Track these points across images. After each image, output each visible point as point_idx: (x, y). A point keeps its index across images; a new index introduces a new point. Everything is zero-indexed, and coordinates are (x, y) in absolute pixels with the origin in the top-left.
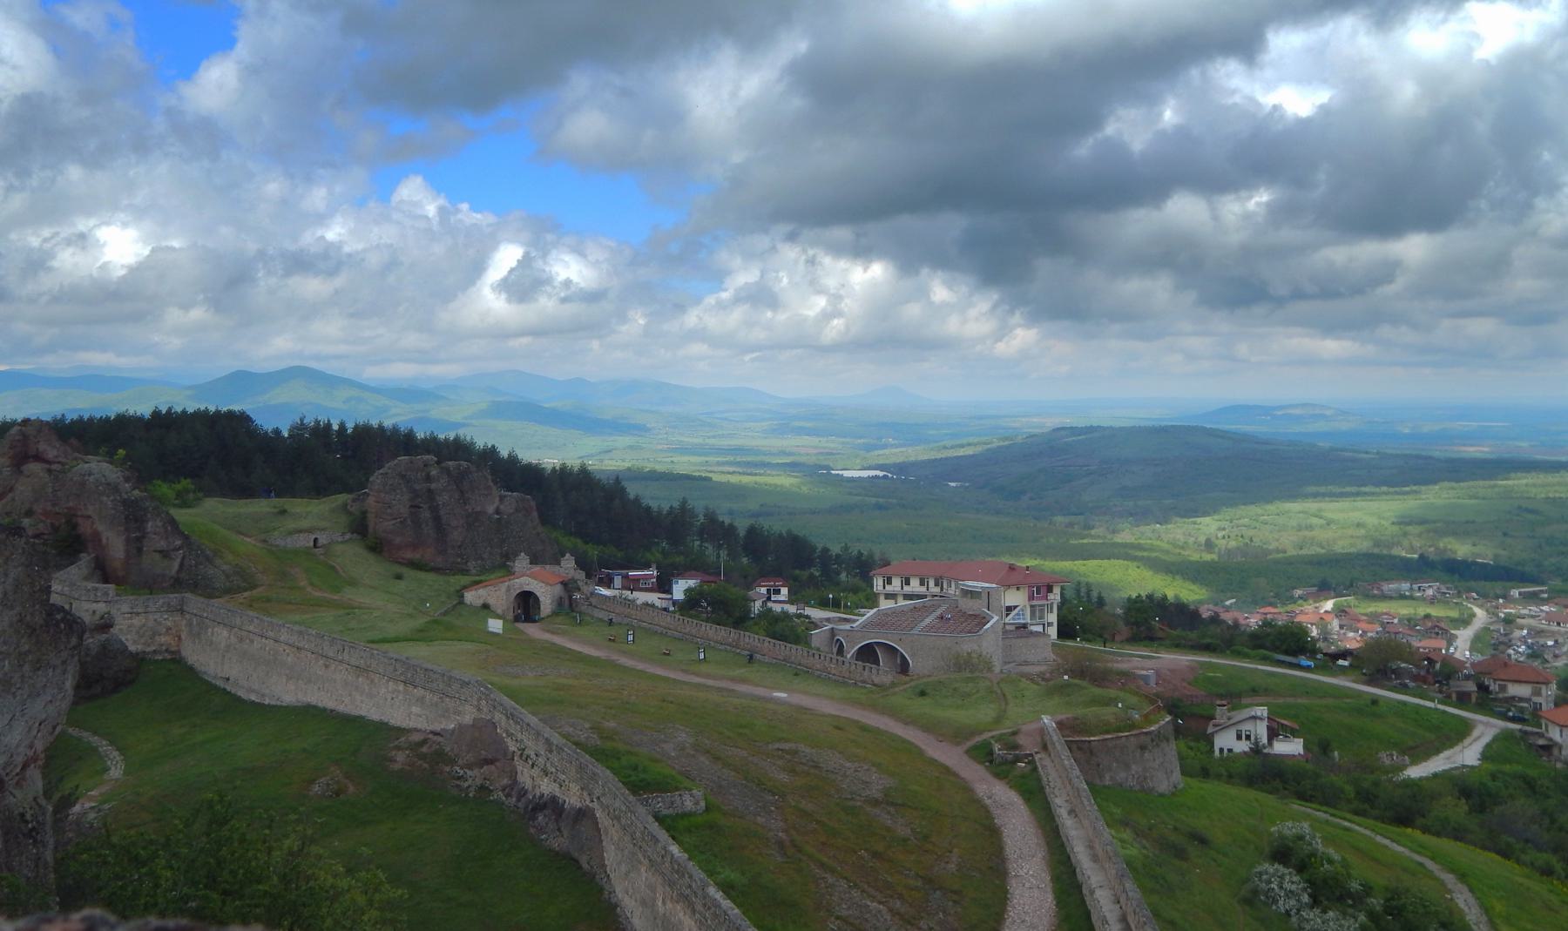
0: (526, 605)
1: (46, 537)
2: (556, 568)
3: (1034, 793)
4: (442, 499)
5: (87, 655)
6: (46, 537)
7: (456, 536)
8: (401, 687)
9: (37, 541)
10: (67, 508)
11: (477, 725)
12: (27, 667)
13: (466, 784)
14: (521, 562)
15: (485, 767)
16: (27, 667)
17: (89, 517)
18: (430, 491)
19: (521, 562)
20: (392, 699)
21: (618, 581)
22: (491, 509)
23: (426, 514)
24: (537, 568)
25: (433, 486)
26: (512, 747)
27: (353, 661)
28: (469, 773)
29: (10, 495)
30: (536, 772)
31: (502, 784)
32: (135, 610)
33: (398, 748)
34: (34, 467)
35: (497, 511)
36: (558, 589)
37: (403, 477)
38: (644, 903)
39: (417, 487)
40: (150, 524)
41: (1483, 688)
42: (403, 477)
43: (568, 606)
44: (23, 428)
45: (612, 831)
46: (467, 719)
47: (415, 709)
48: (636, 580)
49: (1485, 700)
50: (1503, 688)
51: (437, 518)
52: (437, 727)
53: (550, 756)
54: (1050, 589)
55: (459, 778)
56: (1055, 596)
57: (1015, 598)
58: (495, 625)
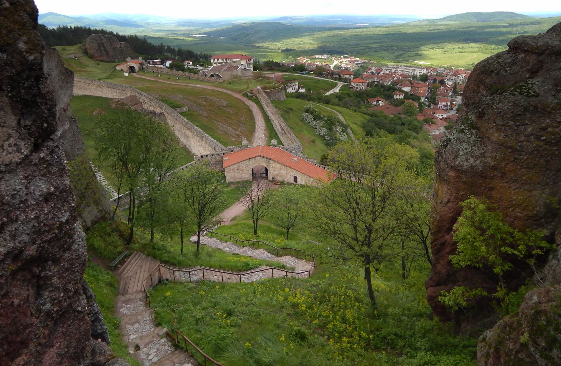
0: (132, 69)
2: (138, 60)
3: (258, 102)
4: (106, 44)
7: (111, 53)
8: (110, 89)
11: (131, 96)
12: (65, 83)
14: (129, 59)
16: (65, 83)
18: (102, 42)
19: (129, 59)
21: (151, 63)
22: (118, 47)
23: (102, 48)
24: (133, 60)
25: (103, 41)
26: (141, 101)
27: (96, 84)
30: (148, 106)
33: (112, 103)
35: (120, 47)
36: (139, 65)
37: (95, 39)
38: (179, 131)
39: (99, 42)
41: (340, 76)
42: (95, 39)
43: (142, 69)
45: (169, 117)
46: (129, 95)
47: (114, 94)
48: (156, 62)
49: (340, 79)
50: (344, 76)
51: (105, 49)
52: (121, 98)
54: (251, 60)
56: (252, 61)
57: (243, 62)
58: (126, 74)
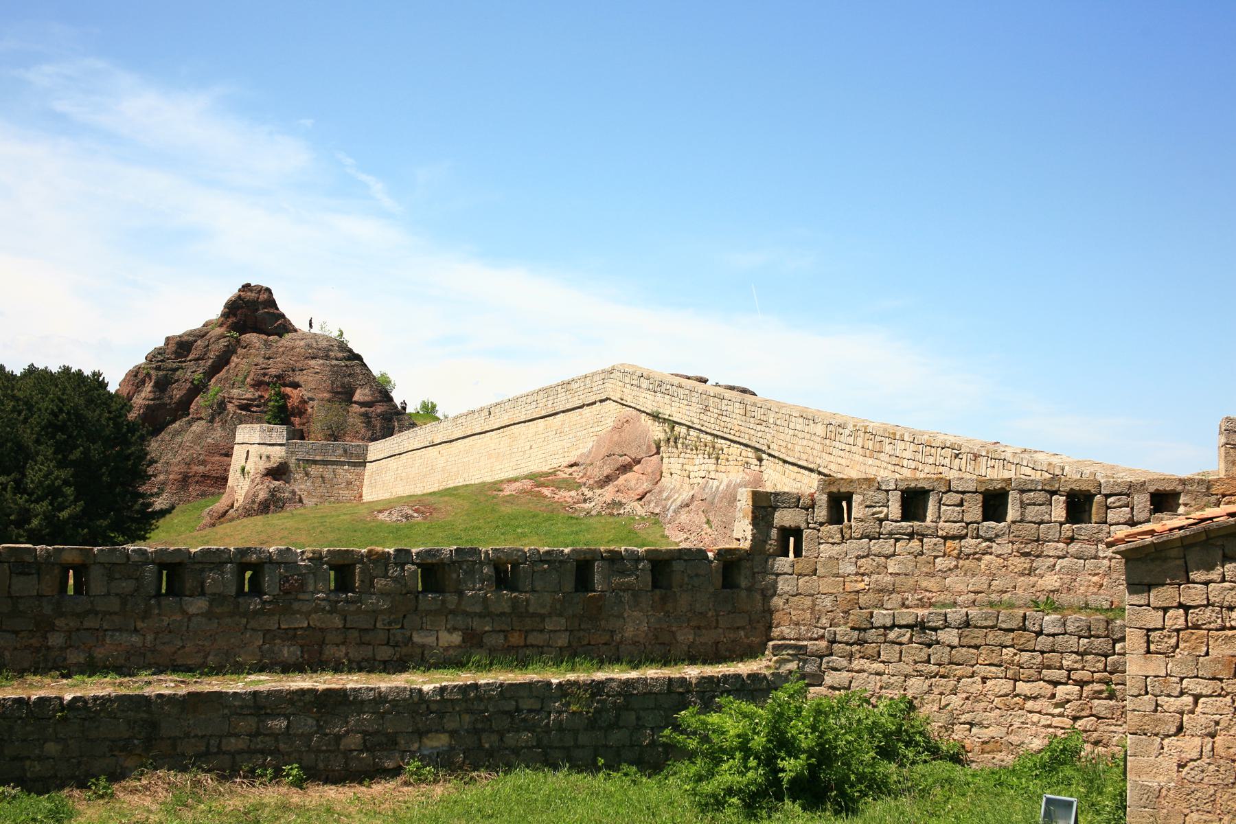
1: (254, 409)
5: (253, 502)
6: (254, 409)
9: (244, 413)
10: (276, 376)
11: (618, 428)
13: (593, 504)
15: (622, 478)
17: (296, 385)
20: (531, 448)
28: (598, 491)
29: (226, 368)
31: (637, 492)
32: (311, 458)
34: (252, 338)
40: (358, 391)
44: (242, 293)
46: (610, 423)
53: (705, 418)
55: (585, 501)
